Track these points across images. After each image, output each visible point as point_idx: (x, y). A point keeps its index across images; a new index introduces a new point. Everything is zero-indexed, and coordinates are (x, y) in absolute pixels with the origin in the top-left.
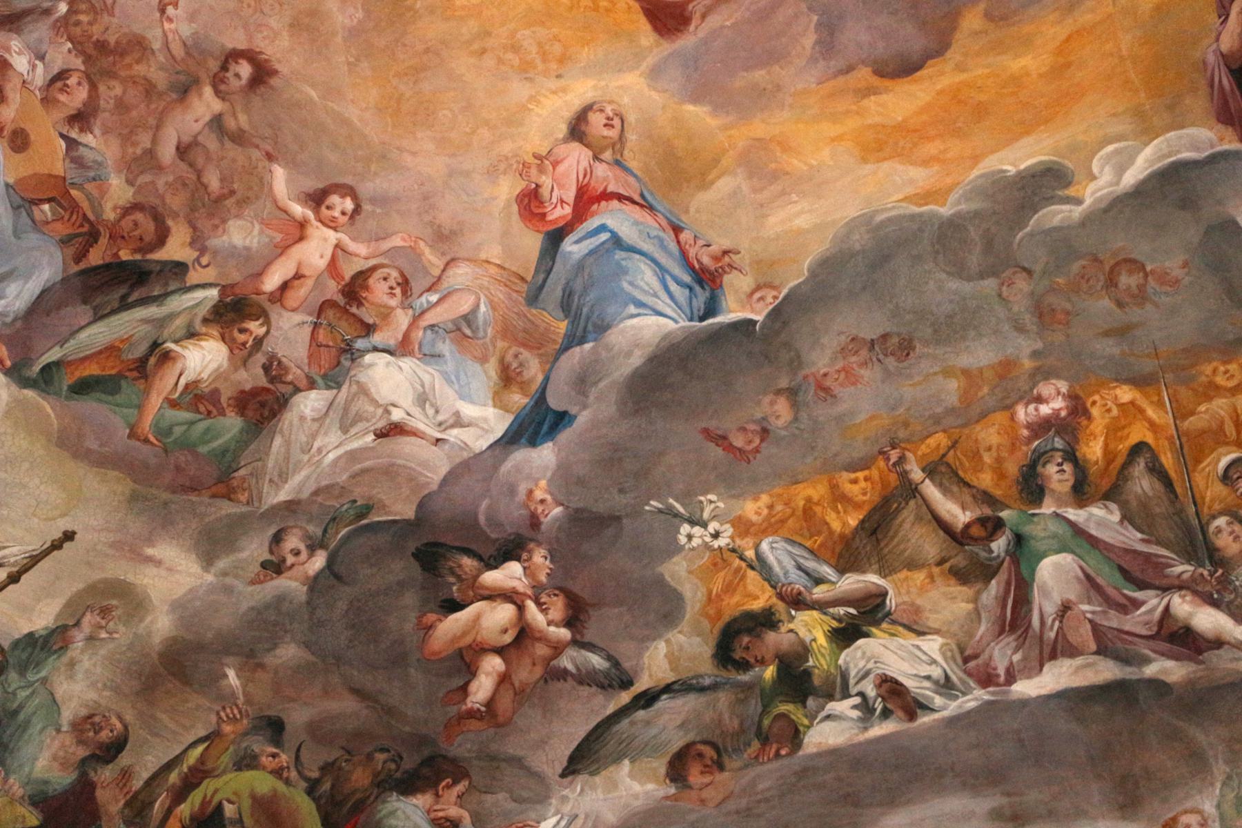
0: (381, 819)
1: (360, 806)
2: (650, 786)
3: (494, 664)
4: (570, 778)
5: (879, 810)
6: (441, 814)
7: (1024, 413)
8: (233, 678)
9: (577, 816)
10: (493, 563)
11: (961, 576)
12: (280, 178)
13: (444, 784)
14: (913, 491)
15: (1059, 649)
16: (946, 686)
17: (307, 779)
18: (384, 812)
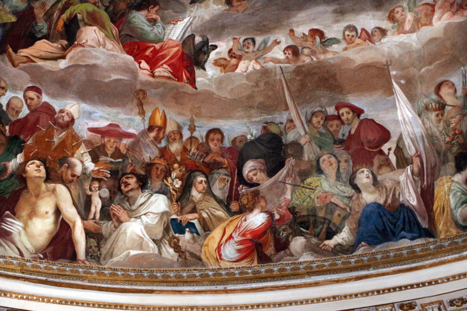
0: (129, 20)
1: (123, 15)
2: (220, 6)
4: (193, 4)
5: (296, 12)
6: (150, 17)
9: (196, 17)
13: (151, 7)
17: (104, 6)
18: (131, 17)
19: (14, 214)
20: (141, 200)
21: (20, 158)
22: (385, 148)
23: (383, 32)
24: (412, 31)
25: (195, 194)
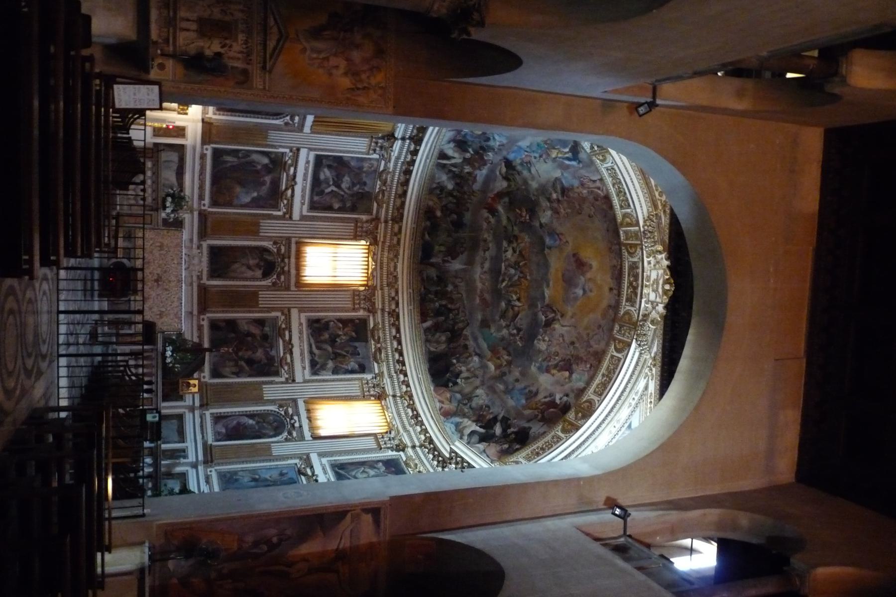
3: (520, 212)
7: (528, 274)
8: (524, 187)
10: (530, 217)
11: (515, 262)
12: (569, 211)
14: (525, 260)
15: (506, 269)
16: (506, 256)
19: (455, 146)
20: (452, 182)
21: (472, 152)
22: (450, 258)
23: (482, 268)
24: (480, 277)
25: (450, 198)
